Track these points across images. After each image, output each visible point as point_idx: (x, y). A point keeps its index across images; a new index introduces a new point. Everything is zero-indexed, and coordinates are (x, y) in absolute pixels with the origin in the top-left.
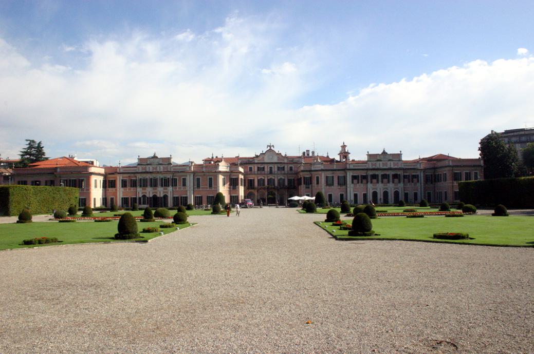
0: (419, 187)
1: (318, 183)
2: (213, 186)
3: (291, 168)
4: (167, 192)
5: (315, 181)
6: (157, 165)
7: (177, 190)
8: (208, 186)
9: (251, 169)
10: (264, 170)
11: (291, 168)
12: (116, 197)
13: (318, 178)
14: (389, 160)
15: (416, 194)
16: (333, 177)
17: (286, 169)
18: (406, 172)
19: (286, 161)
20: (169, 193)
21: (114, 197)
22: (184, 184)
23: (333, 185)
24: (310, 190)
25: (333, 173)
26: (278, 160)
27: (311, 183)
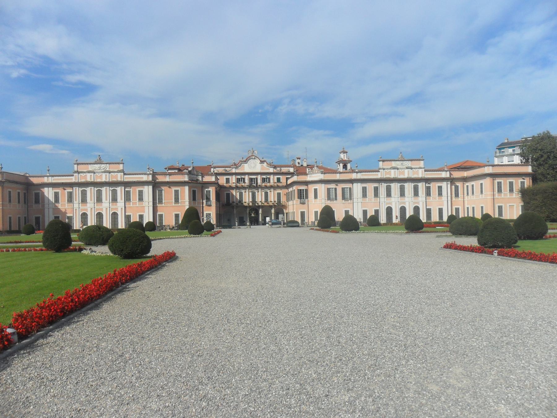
0: (445, 203)
1: (316, 197)
2: (180, 201)
3: (279, 180)
4: (117, 209)
5: (311, 194)
6: (102, 172)
7: (131, 205)
8: (174, 201)
9: (228, 180)
10: (244, 182)
11: (279, 180)
12: (44, 216)
13: (316, 190)
14: (407, 168)
15: (441, 211)
16: (336, 189)
17: (272, 181)
18: (429, 183)
19: (271, 170)
20: (119, 209)
21: (41, 216)
22: (141, 199)
23: (336, 199)
24: (306, 205)
25: (337, 185)
26: (262, 169)
27: (307, 197)
